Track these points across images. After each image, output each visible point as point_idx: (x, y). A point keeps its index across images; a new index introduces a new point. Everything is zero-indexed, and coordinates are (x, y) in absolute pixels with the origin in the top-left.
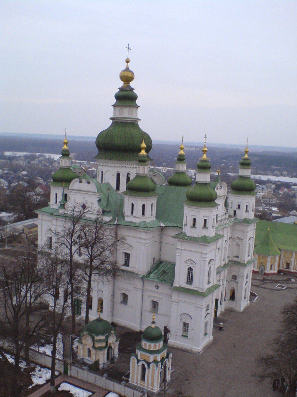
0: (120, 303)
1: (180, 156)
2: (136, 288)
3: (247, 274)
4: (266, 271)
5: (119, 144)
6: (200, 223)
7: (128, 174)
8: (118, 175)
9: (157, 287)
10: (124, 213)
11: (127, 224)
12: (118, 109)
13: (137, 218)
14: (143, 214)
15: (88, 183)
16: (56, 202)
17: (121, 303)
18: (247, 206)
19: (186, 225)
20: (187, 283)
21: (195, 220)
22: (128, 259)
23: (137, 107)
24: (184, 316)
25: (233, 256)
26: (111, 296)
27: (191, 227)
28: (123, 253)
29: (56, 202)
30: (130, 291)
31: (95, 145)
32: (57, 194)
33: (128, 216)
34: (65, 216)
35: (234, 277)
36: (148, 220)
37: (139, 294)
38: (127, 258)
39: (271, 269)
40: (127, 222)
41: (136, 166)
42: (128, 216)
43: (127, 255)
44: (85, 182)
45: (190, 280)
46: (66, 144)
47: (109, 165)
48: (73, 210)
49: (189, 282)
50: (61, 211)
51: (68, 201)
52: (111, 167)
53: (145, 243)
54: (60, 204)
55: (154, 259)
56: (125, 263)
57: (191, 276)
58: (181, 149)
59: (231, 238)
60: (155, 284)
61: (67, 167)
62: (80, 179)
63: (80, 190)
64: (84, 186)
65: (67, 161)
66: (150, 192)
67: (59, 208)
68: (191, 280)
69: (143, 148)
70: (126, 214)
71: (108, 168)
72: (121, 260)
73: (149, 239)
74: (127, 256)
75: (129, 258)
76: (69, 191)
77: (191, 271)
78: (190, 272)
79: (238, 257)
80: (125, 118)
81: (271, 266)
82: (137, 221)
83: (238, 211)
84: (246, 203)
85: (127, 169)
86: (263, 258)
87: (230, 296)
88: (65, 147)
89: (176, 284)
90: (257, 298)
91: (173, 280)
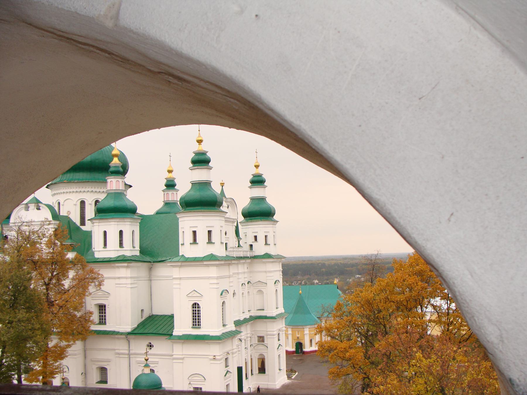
0: (96, 383)
2: (119, 354)
3: (279, 334)
4: (305, 349)
6: (202, 237)
7: (97, 202)
9: (151, 346)
10: (94, 248)
14: (121, 245)
18: (266, 236)
19: (183, 244)
20: (193, 328)
21: (194, 233)
24: (195, 378)
25: (256, 310)
26: (82, 373)
27: (191, 244)
28: (96, 305)
35: (261, 339)
36: (128, 254)
39: (311, 345)
43: (102, 308)
44: (34, 209)
45: (196, 321)
49: (196, 325)
52: (71, 194)
56: (100, 322)
57: (198, 316)
59: (250, 283)
60: (147, 343)
68: (198, 322)
74: (102, 310)
75: (105, 313)
77: (197, 309)
78: (196, 311)
79: (263, 310)
81: (311, 341)
82: (113, 255)
83: (255, 245)
84: (265, 232)
85: (96, 194)
86: (298, 332)
87: (259, 369)
89: (177, 331)
90: (297, 373)
91: (173, 327)
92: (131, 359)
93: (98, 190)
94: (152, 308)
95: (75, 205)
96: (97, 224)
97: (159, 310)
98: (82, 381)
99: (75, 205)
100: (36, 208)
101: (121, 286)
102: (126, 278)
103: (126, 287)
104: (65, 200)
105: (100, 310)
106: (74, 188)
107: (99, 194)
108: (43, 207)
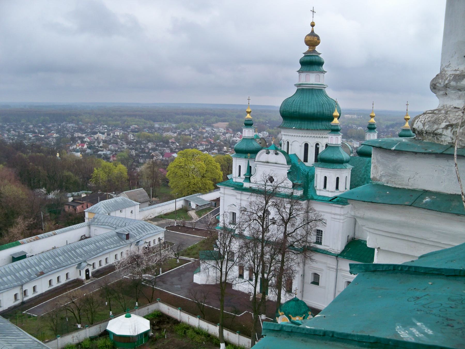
0: (311, 283)
1: (370, 124)
5: (306, 112)
7: (317, 144)
8: (306, 145)
10: (316, 187)
11: (319, 198)
12: (303, 75)
13: (330, 192)
14: (337, 188)
15: (277, 154)
16: (240, 175)
17: (312, 283)
22: (320, 237)
23: (323, 72)
29: (240, 175)
30: (322, 270)
31: (279, 114)
32: (240, 166)
33: (320, 190)
34: (251, 190)
37: (333, 274)
38: (319, 235)
40: (320, 196)
41: (328, 136)
42: (320, 190)
43: (319, 233)
46: (249, 113)
47: (296, 135)
48: (266, 183)
50: (246, 185)
51: (252, 173)
52: (298, 137)
53: (339, 219)
54: (244, 177)
55: (348, 236)
56: (317, 241)
58: (372, 117)
61: (251, 138)
62: (268, 150)
63: (268, 162)
64: (272, 157)
65: (251, 130)
66: (344, 164)
67: (243, 181)
69: (336, 116)
70: (318, 188)
71: (296, 139)
72: (313, 238)
73: (343, 215)
74: (319, 233)
75: (321, 236)
76: (255, 163)
80: (312, 84)
88: (248, 116)
92: (338, 273)
93: (318, 136)
94: (355, 233)
95: (300, 146)
96: (320, 170)
97: (359, 236)
98: (301, 280)
99: (300, 146)
100: (274, 153)
101: (335, 220)
102: (340, 215)
103: (339, 221)
104: (293, 141)
105: (317, 233)
106: (301, 133)
107: (319, 139)
108: (280, 154)
